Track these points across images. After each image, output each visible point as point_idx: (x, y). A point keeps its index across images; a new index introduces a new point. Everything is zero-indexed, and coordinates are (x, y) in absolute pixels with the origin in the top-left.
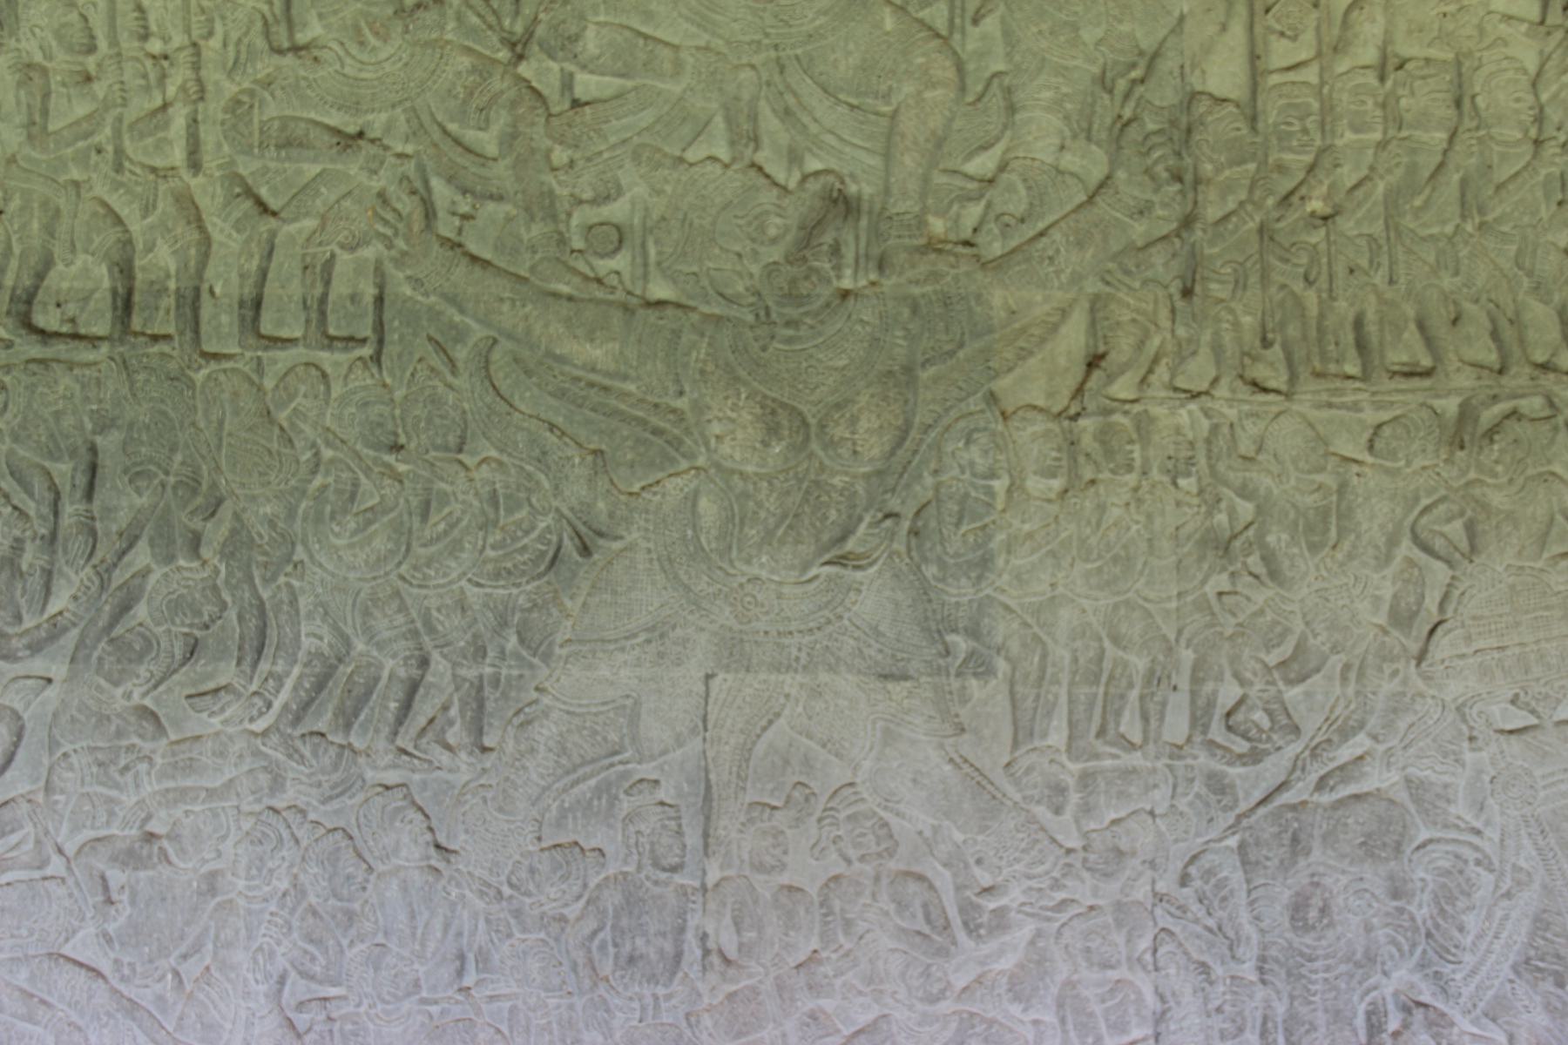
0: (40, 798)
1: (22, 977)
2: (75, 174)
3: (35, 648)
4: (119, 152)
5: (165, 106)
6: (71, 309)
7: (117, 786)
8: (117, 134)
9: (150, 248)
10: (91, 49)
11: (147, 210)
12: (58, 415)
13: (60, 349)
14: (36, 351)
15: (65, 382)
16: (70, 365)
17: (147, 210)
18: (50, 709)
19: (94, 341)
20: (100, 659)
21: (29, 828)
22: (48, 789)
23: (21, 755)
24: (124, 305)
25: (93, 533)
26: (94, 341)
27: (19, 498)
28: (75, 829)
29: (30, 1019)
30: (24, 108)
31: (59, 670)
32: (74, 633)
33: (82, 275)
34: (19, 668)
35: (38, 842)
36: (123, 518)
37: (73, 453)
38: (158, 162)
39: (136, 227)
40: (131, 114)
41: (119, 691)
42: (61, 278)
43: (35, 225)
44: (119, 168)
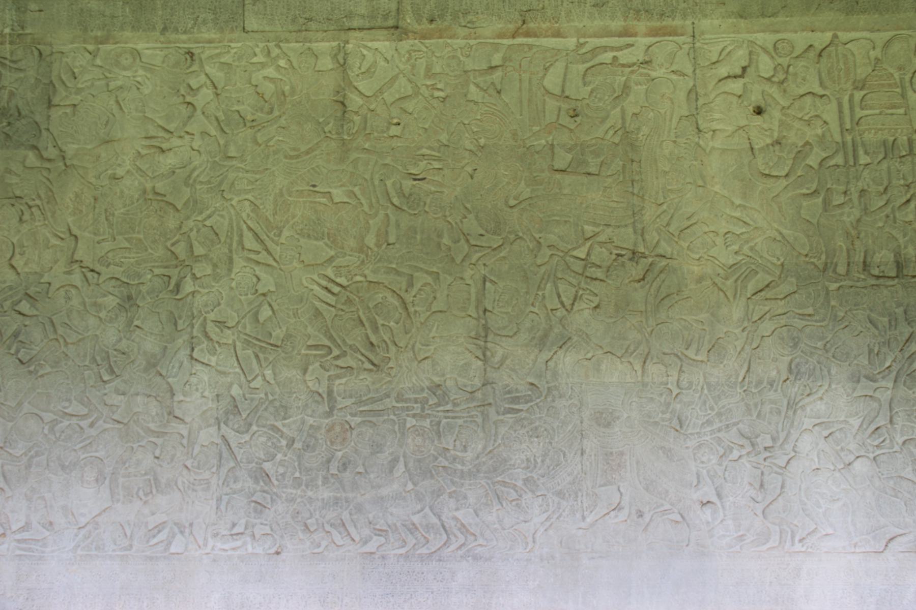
0: (889, 426)
1: (891, 483)
2: (881, 224)
3: (883, 378)
4: (895, 217)
5: (908, 201)
6: (882, 268)
7: (914, 422)
8: (893, 211)
9: (905, 247)
10: (882, 184)
11: (905, 236)
12: (884, 303)
13: (881, 281)
14: (874, 282)
15: (885, 292)
16: (887, 287)
17: (905, 236)
18: (889, 397)
19: (893, 278)
20: (905, 381)
21: (887, 435)
22: (891, 421)
23: (881, 412)
24: (899, 266)
25: (897, 340)
26: (893, 278)
27: (873, 330)
28: (902, 436)
29: (896, 496)
30: (863, 204)
31: (890, 385)
32: (894, 373)
33: (883, 257)
34: (876, 385)
35: (891, 440)
36: (907, 335)
37: (890, 315)
38: (907, 220)
39: (901, 241)
40: (898, 204)
41: (911, 392)
42: (877, 258)
43: (870, 241)
44: (895, 222)
